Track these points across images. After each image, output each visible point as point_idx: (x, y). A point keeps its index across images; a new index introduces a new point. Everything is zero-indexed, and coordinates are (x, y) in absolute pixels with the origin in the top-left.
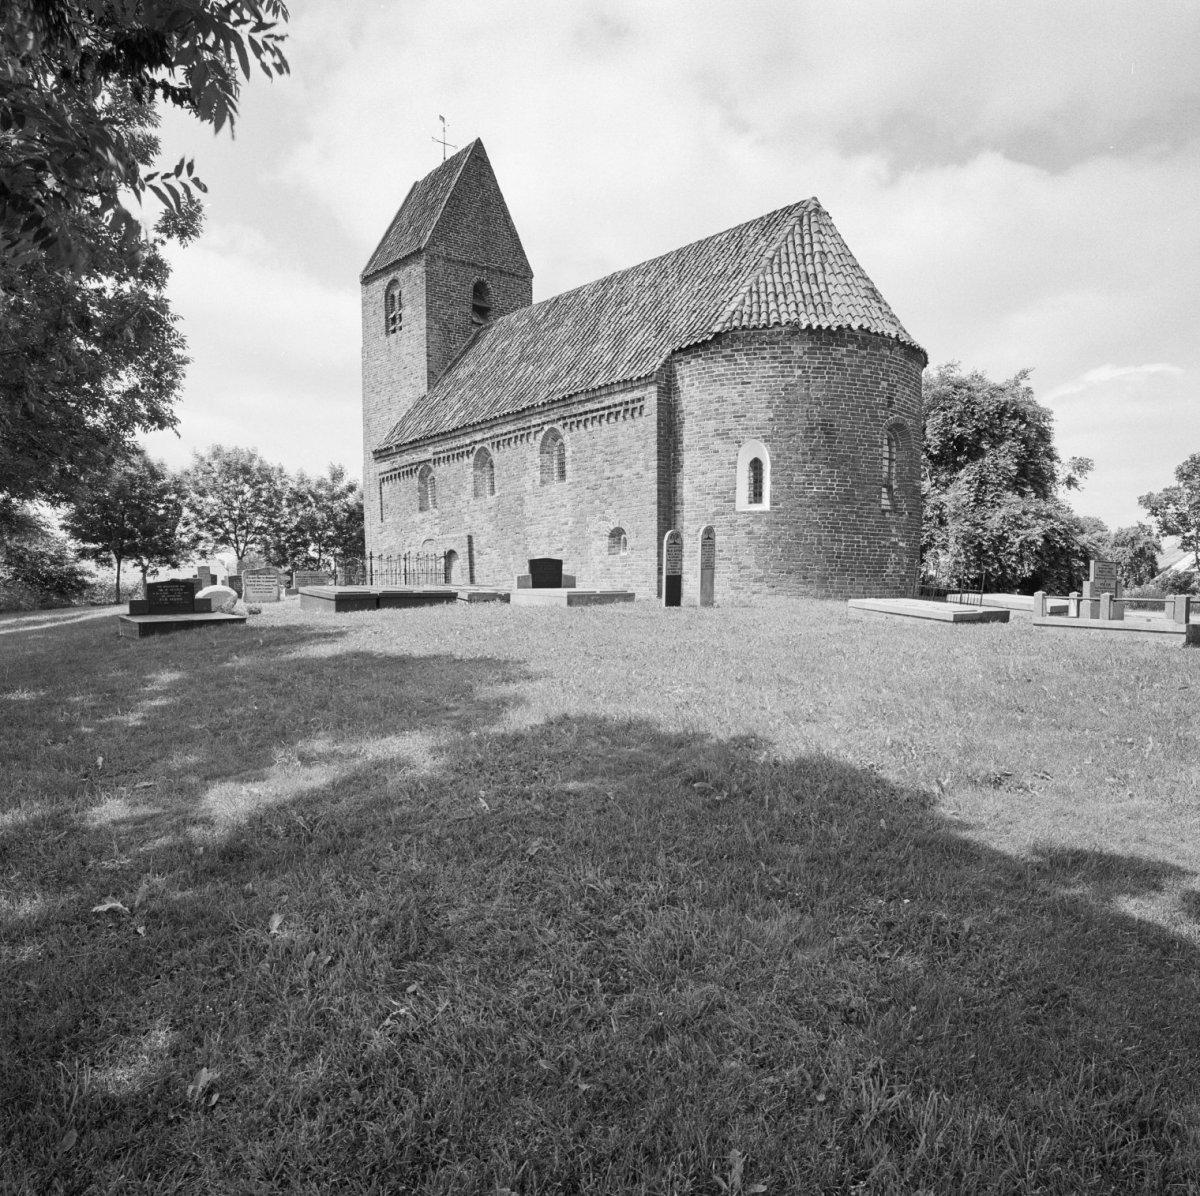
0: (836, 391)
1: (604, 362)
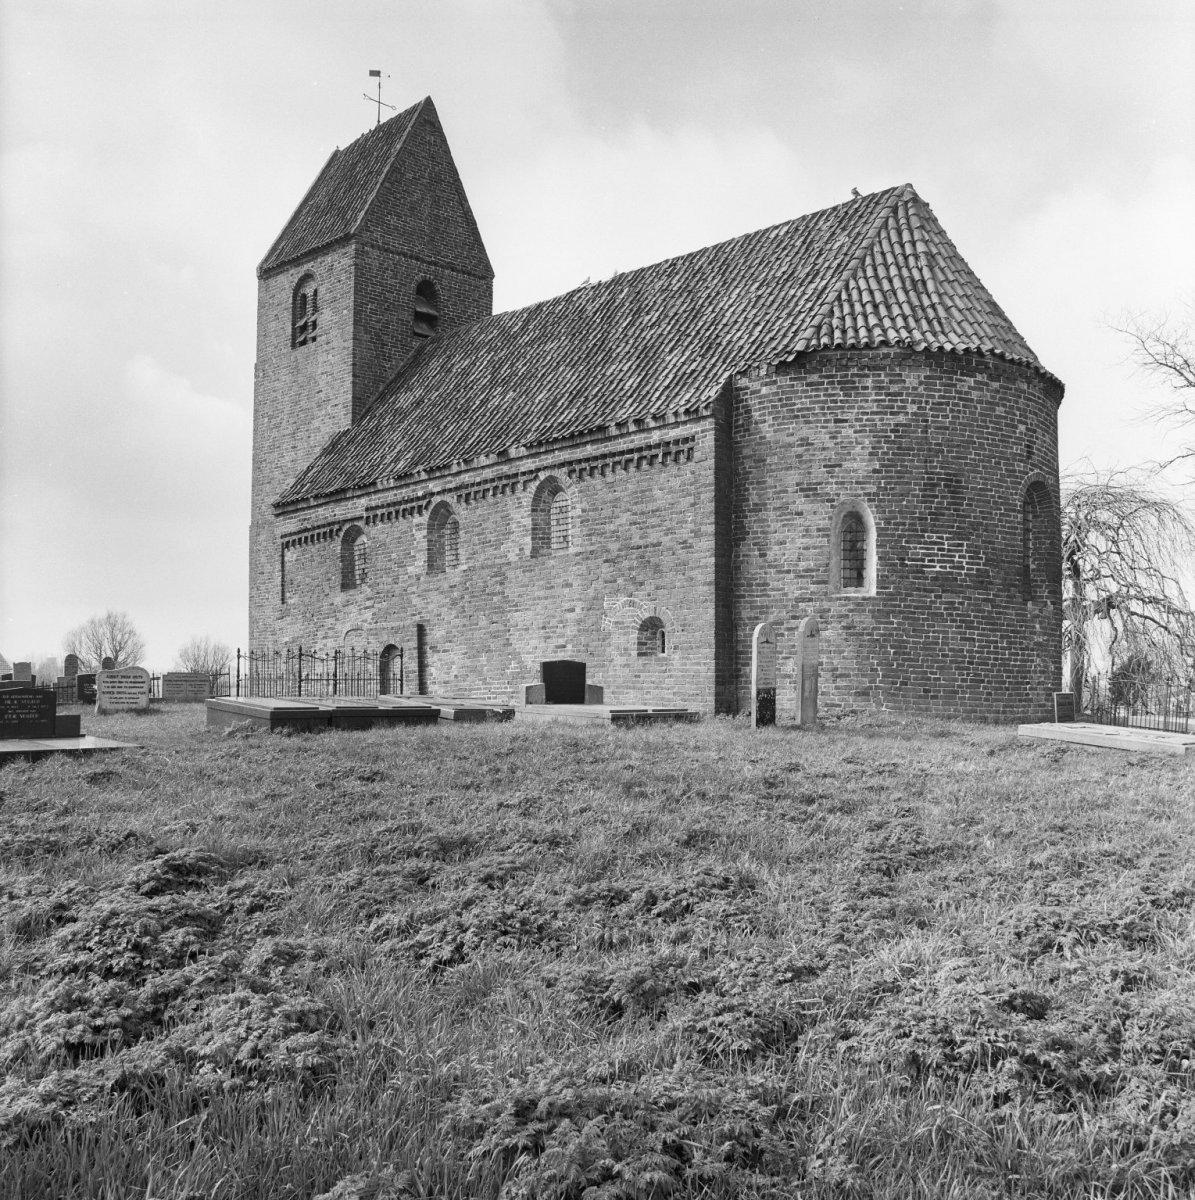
0: (963, 436)
1: (626, 388)
